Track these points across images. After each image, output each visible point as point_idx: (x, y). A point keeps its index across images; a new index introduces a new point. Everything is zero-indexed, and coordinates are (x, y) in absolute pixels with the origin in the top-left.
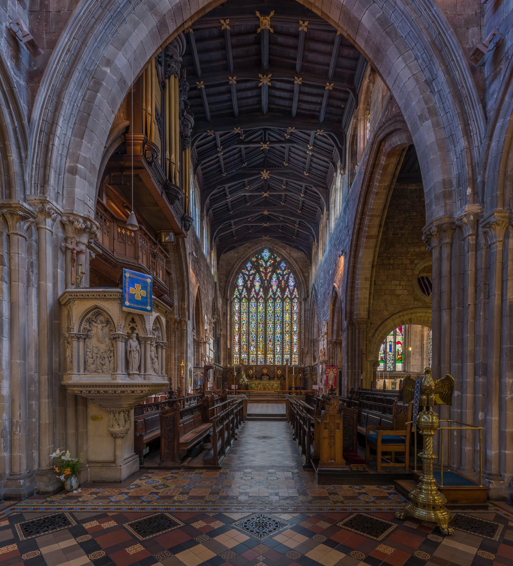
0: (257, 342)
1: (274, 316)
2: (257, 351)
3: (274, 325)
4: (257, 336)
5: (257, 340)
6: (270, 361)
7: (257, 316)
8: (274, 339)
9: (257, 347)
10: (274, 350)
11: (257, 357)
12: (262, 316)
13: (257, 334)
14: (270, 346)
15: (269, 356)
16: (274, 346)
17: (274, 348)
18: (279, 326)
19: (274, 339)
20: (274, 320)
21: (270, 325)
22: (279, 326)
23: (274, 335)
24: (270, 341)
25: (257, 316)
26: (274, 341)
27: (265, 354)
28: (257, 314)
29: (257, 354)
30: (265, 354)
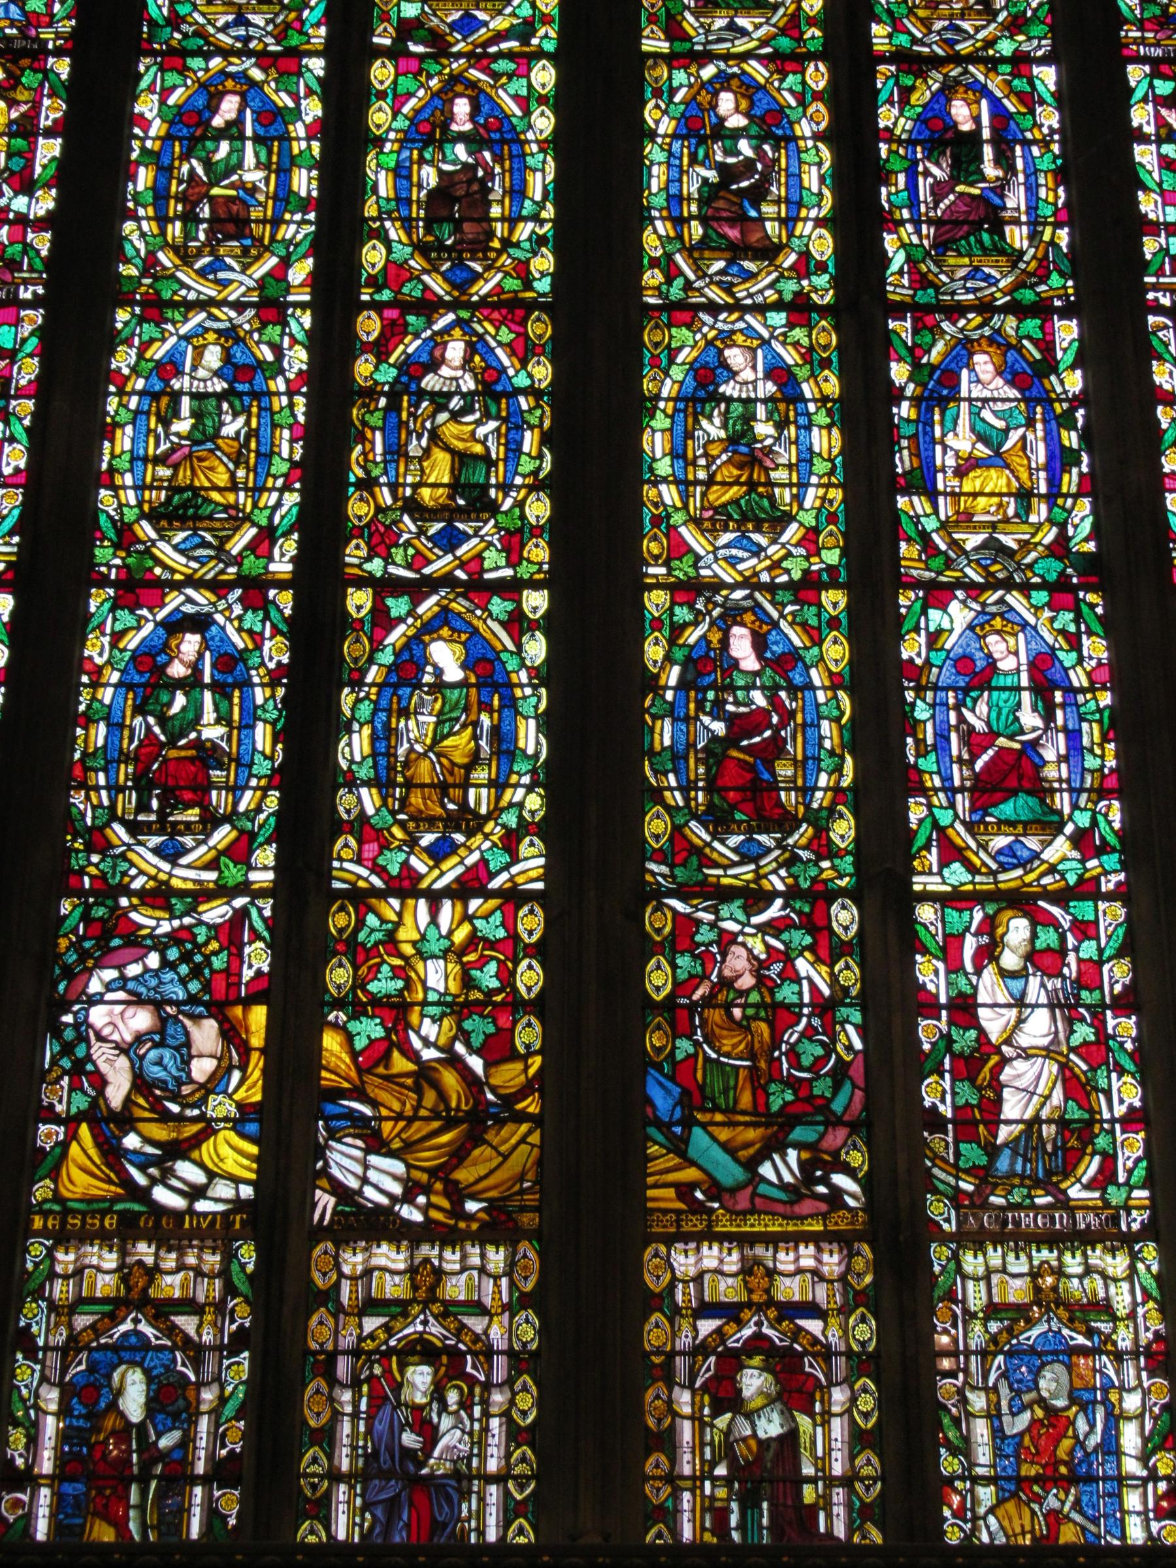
0: (307, 823)
1: (852, 133)
2: (290, 1122)
3: (863, 355)
4: (318, 633)
5: (307, 774)
6: (769, 1472)
7: (345, 138)
8: (879, 727)
9: (296, 999)
10: (894, 1060)
11: (280, 1309)
12: (495, 134)
13: (320, 576)
14: (747, 937)
15: (704, 1265)
16: (891, 936)
17: (891, 1000)
18: (983, 377)
19: (879, 727)
20: (858, 219)
21: (742, 350)
22: (983, 377)
23: (874, 630)
24: (744, 790)
25: (345, 138)
26: (883, 784)
27: (588, 1237)
28: (346, 95)
29: (280, 1218)
30: (588, 1237)
